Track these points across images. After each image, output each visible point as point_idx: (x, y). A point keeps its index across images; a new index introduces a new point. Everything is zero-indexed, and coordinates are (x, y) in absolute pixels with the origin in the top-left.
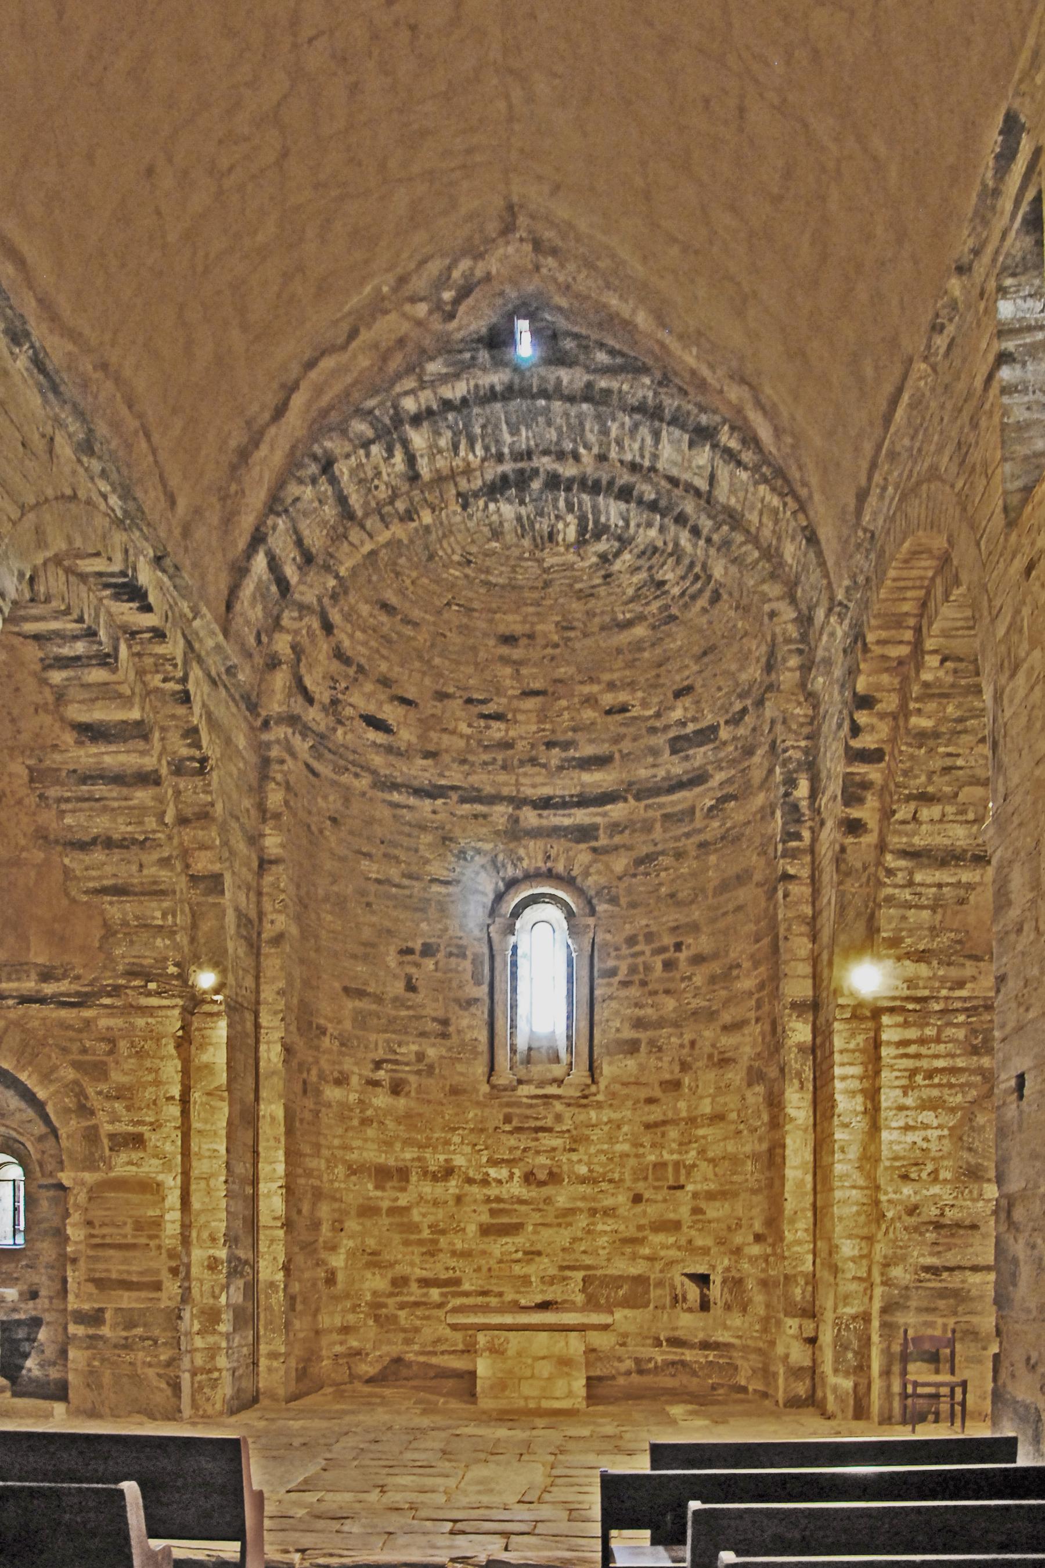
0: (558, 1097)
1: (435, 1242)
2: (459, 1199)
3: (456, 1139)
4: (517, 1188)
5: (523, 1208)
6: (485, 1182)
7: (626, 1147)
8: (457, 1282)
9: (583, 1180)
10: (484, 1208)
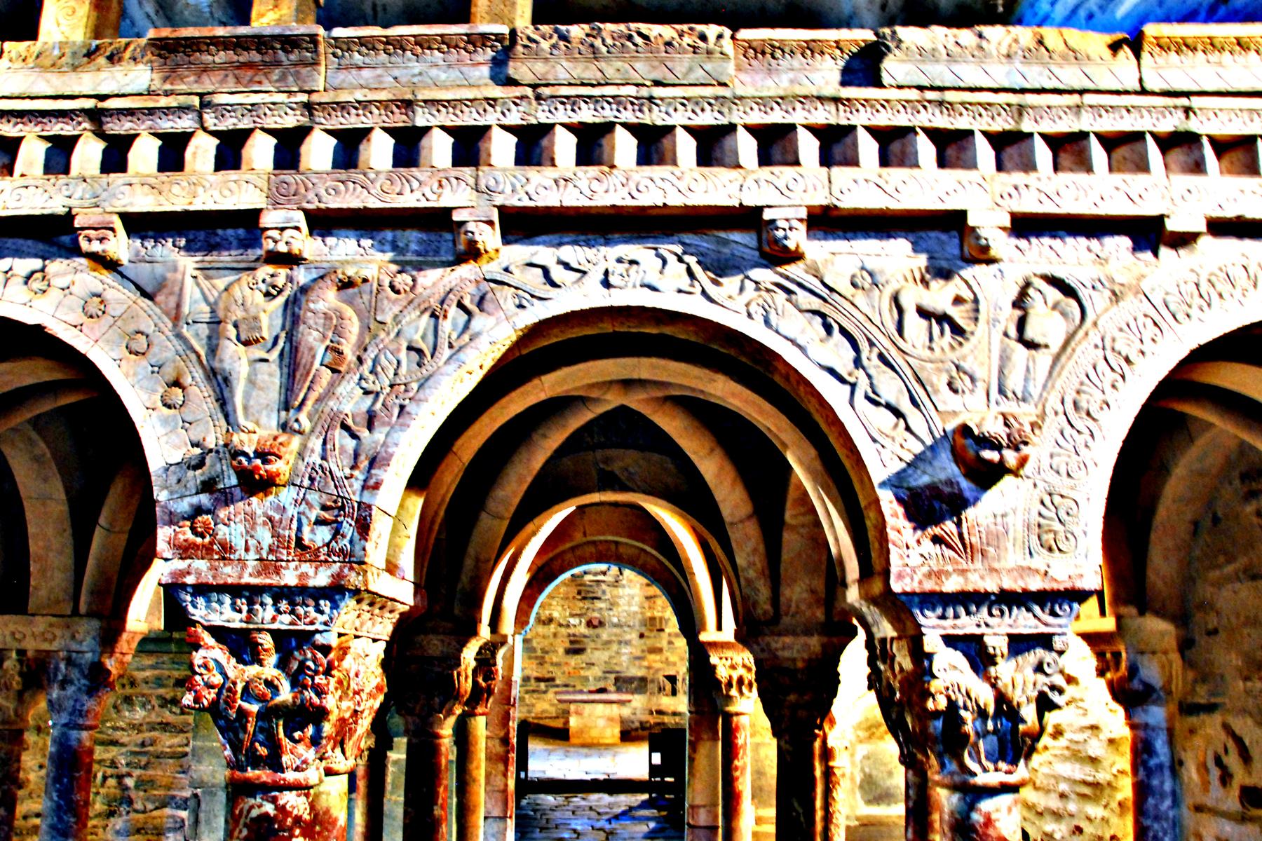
1: (543, 658)
2: (555, 635)
3: (554, 603)
4: (583, 629)
6: (568, 626)
7: (635, 608)
8: (553, 679)
9: (616, 626)
10: (567, 640)
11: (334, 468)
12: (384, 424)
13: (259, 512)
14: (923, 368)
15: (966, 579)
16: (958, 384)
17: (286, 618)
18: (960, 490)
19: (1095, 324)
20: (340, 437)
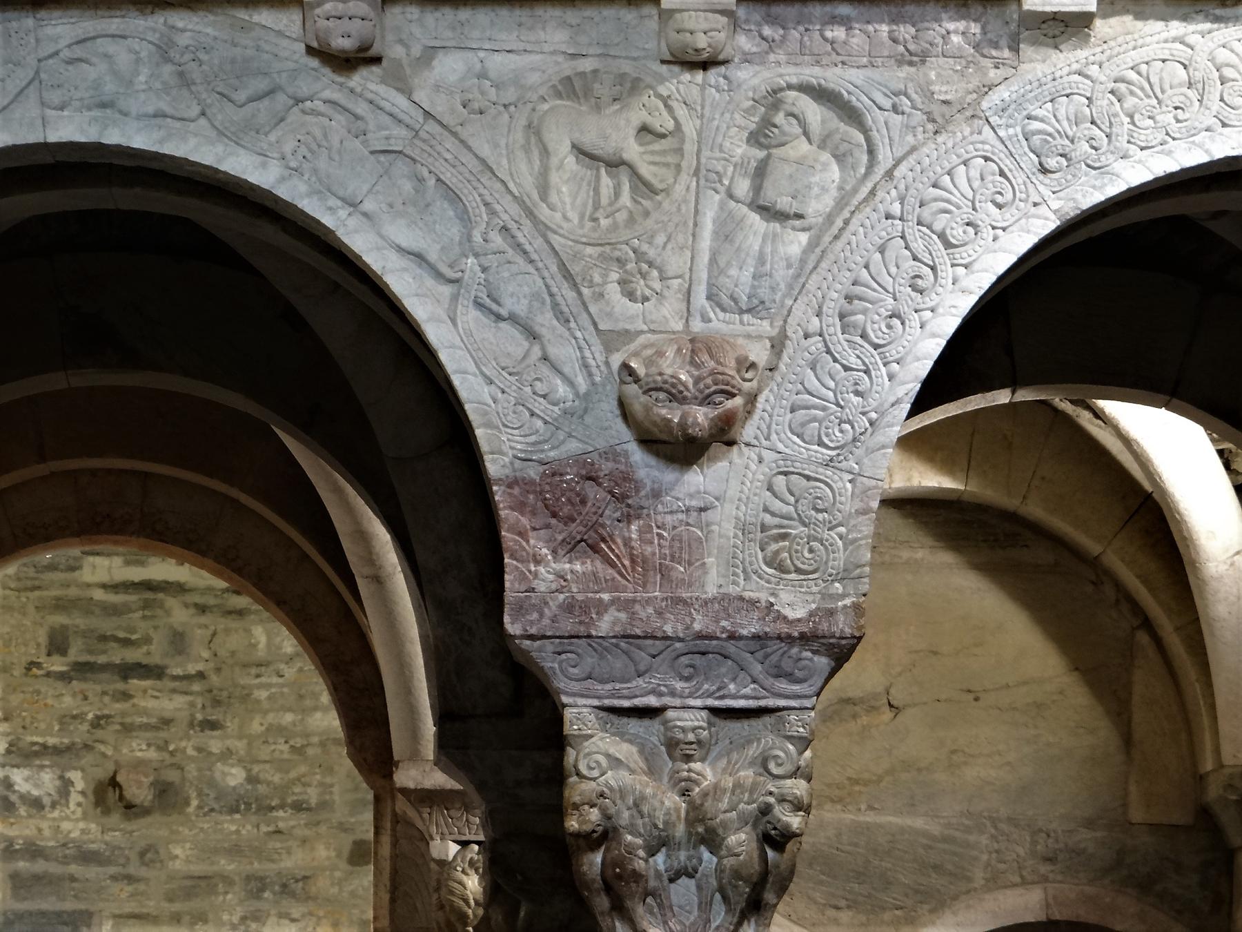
0: (178, 589)
5: (92, 872)
9: (236, 804)
14: (576, 256)
15: (633, 616)
16: (640, 287)
18: (628, 464)
19: (889, 174)
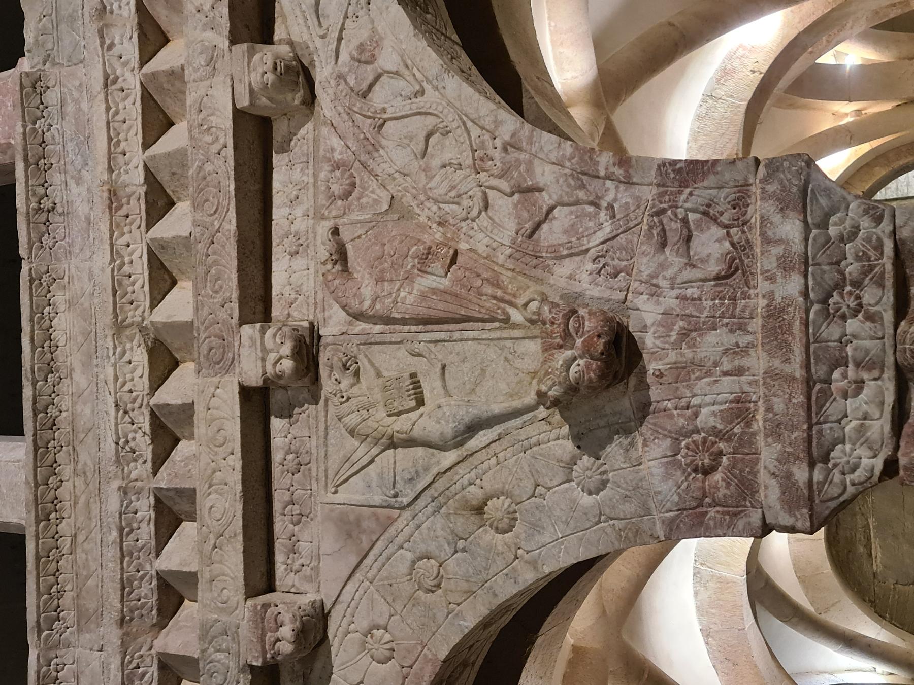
11: (600, 236)
12: (530, 169)
13: (672, 356)
17: (869, 296)
20: (551, 234)
